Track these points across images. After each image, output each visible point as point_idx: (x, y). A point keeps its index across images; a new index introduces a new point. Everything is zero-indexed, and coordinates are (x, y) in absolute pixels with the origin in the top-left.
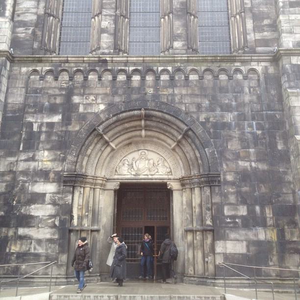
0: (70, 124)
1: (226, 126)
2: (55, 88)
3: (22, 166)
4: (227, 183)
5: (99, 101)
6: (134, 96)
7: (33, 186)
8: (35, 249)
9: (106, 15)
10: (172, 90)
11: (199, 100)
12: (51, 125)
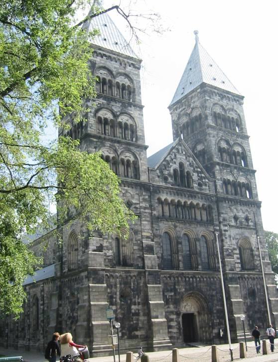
3: (167, 310)
6: (191, 286)
12: (171, 296)
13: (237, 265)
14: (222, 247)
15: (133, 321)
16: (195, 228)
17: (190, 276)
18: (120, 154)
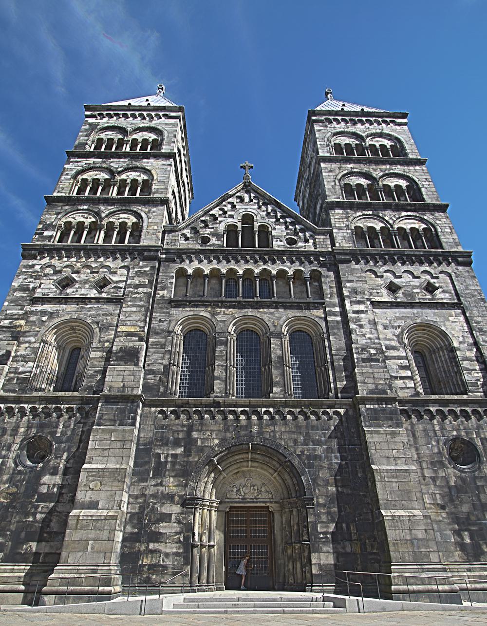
0: (190, 455)
1: (318, 457)
2: (178, 425)
3: (151, 491)
4: (319, 505)
5: (214, 436)
6: (243, 433)
7: (161, 507)
8: (163, 561)
9: (218, 366)
10: (272, 428)
11: (296, 436)
12: (175, 456)
13: (399, 383)
14: (349, 342)
15: (34, 515)
16: (272, 313)
17: (240, 409)
18: (107, 216)
